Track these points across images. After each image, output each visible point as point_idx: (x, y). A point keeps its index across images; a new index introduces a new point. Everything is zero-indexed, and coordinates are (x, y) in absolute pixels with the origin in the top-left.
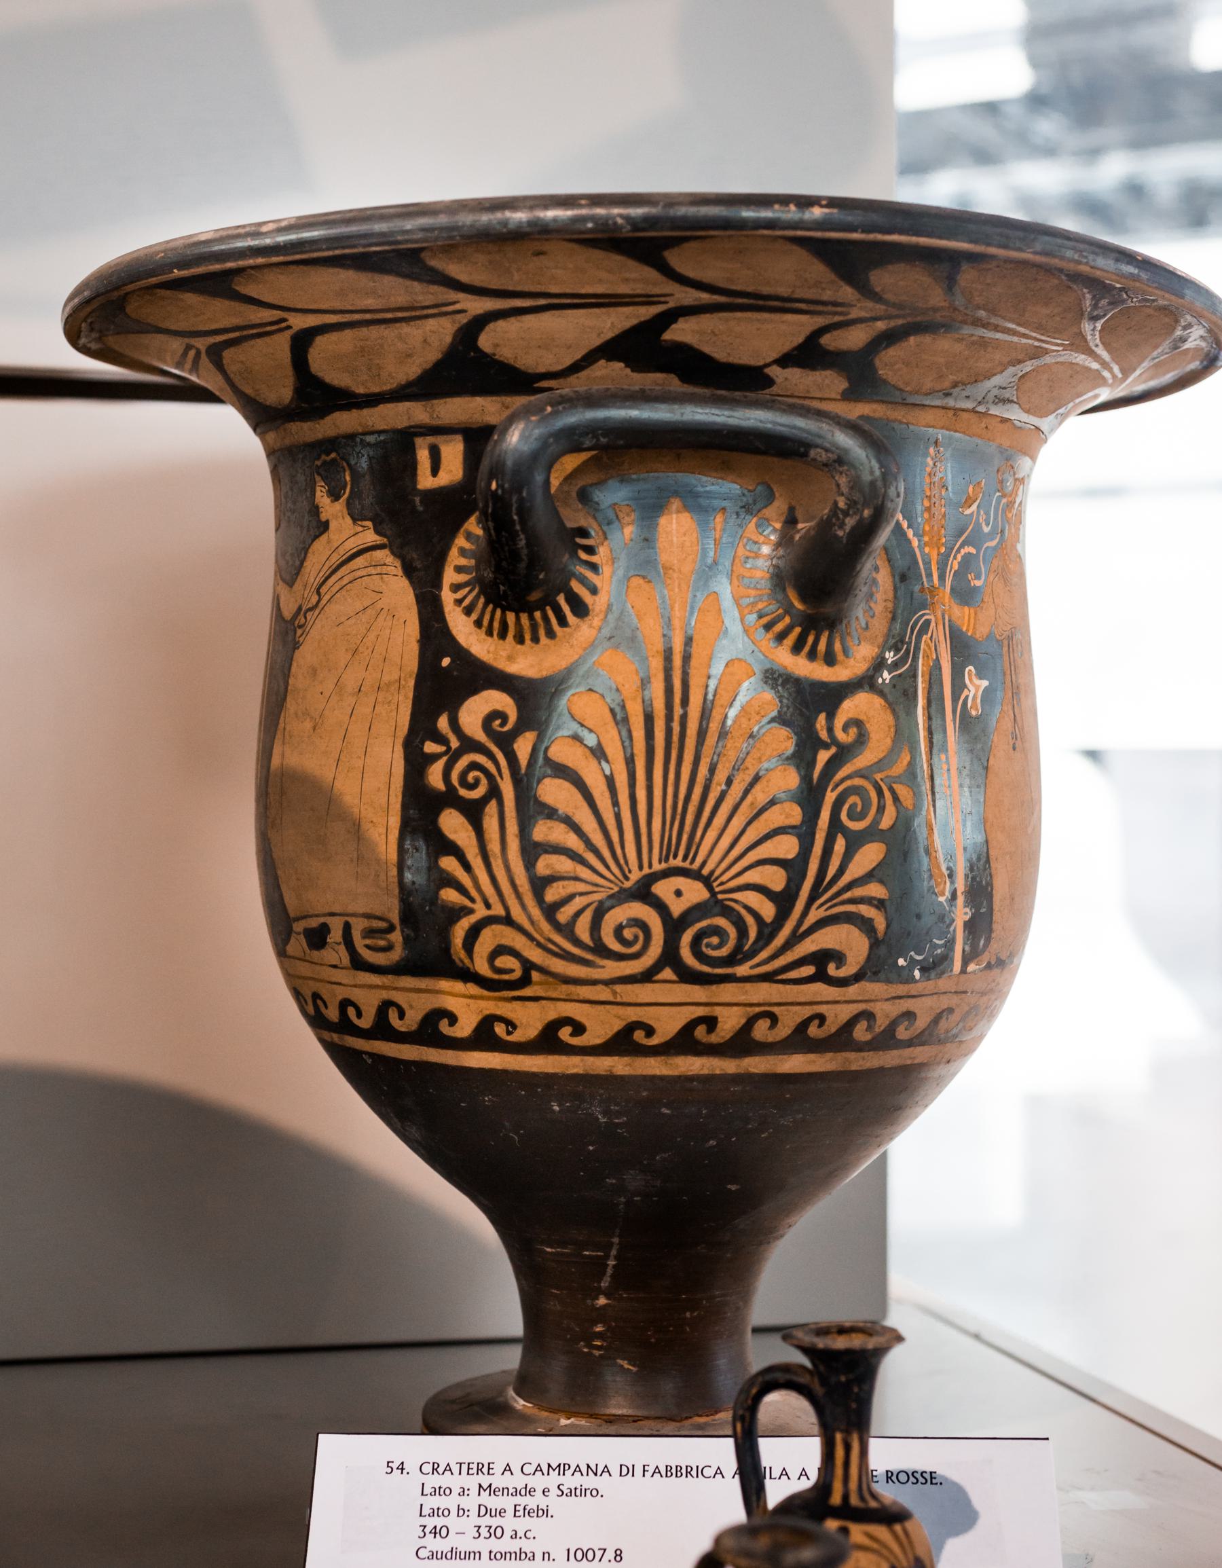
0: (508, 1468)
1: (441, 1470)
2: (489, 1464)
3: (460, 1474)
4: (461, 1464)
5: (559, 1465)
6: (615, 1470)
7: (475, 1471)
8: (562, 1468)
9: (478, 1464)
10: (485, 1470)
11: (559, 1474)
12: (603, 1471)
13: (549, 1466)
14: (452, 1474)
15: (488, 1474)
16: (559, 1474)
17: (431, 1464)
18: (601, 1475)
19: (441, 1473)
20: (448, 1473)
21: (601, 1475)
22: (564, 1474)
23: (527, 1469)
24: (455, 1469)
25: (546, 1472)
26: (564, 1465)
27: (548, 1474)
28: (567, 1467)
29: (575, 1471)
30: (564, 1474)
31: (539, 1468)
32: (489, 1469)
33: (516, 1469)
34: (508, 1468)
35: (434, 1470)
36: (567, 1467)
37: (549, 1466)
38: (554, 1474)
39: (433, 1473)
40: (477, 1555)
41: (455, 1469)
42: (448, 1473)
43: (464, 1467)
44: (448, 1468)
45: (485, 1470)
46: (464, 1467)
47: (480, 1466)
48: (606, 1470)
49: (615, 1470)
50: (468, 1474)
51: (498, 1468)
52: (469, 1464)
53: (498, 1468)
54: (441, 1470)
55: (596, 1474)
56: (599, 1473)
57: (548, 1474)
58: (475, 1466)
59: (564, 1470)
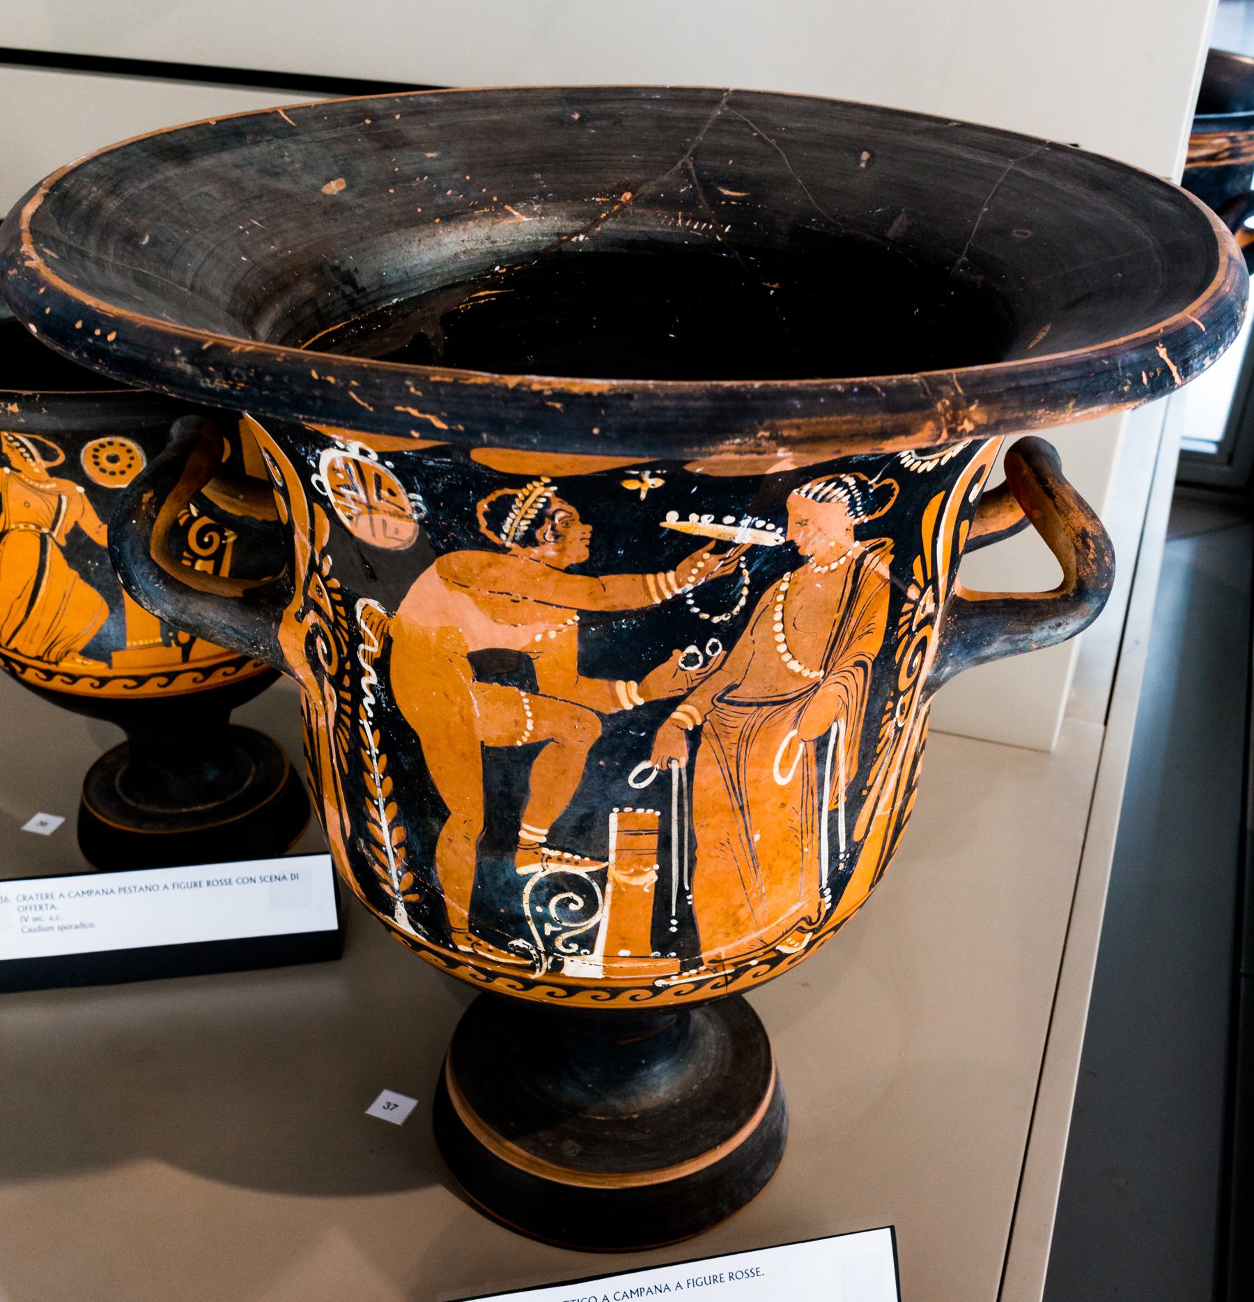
6: (116, 890)
23: (71, 895)
24: (34, 897)
33: (66, 895)
35: (24, 899)
40: (51, 928)
41: (34, 897)
43: (39, 897)
44: (31, 897)
49: (116, 890)
51: (56, 895)
53: (56, 895)
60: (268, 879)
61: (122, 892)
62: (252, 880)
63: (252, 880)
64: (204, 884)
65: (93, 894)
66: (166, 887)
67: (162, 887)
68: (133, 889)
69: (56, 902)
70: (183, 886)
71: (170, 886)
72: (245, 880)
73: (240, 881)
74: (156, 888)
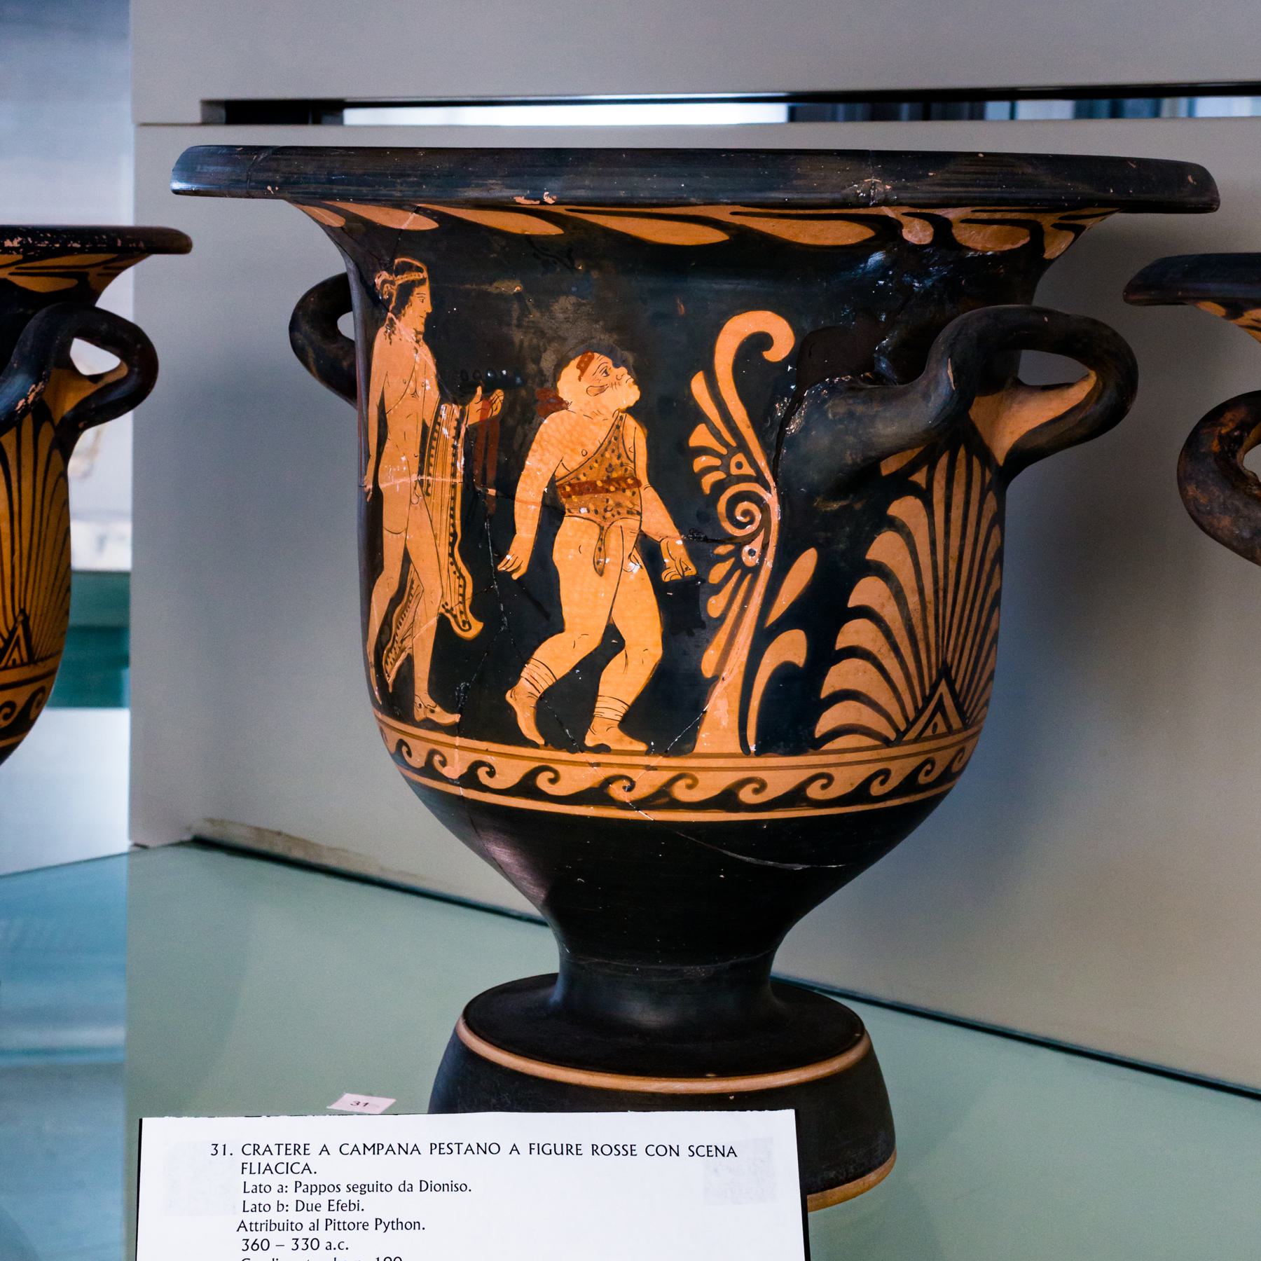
2: (305, 1145)
5: (374, 1146)
6: (424, 1148)
7: (292, 1151)
11: (374, 1154)
13: (365, 1146)
16: (374, 1154)
22: (378, 1154)
23: (346, 1149)
26: (378, 1145)
27: (364, 1154)
29: (388, 1150)
30: (378, 1154)
32: (305, 1149)
33: (334, 1149)
34: (325, 1149)
37: (365, 1146)
43: (283, 1148)
48: (416, 1149)
49: (424, 1148)
51: (314, 1149)
57: (364, 1154)
58: (292, 1147)
59: (378, 1150)
60: (703, 1151)
62: (673, 1151)
63: (673, 1151)
64: (587, 1150)
65: (382, 1152)
66: (515, 1148)
67: (506, 1148)
68: (455, 1148)
69: (313, 1159)
71: (524, 1149)
72: (661, 1150)
73: (652, 1150)
74: (495, 1149)
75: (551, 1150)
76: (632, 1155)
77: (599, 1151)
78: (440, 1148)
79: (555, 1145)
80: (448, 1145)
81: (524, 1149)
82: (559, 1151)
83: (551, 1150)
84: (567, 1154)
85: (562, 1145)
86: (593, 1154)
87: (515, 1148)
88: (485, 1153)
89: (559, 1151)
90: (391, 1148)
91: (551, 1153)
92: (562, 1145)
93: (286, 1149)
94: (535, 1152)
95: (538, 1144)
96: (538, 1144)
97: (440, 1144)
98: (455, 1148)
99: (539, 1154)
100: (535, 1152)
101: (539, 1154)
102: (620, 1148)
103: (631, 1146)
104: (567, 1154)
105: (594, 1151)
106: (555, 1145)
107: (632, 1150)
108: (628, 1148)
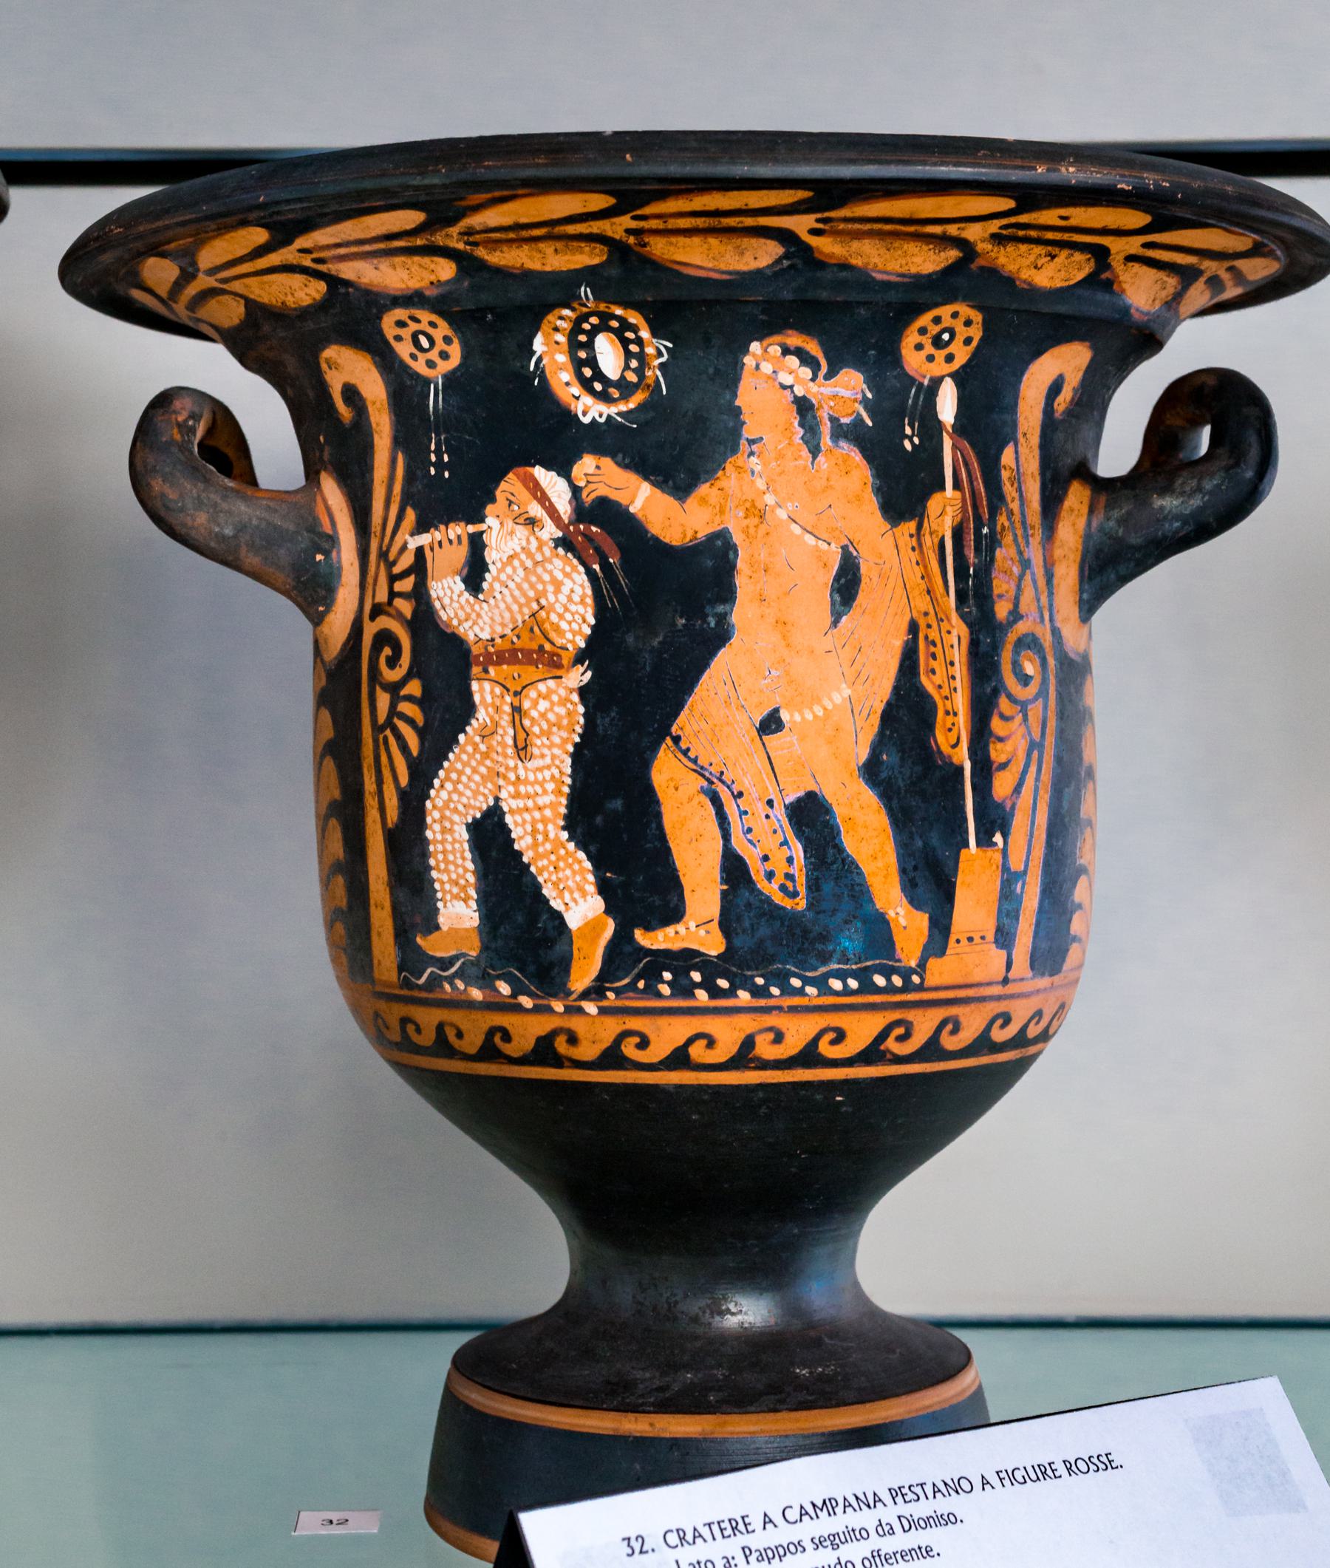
0: (767, 1520)
1: (689, 1537)
2: (743, 1518)
3: (714, 1539)
4: (709, 1525)
5: (824, 1502)
7: (729, 1532)
8: (828, 1505)
9: (730, 1520)
10: (741, 1527)
12: (875, 1502)
13: (814, 1505)
14: (705, 1541)
15: (748, 1532)
16: (830, 1515)
17: (675, 1533)
18: (875, 1506)
19: (691, 1541)
20: (699, 1541)
21: (875, 1506)
24: (705, 1532)
25: (814, 1515)
26: (830, 1500)
27: (818, 1517)
28: (834, 1504)
29: (845, 1507)
30: (835, 1513)
31: (803, 1513)
32: (746, 1525)
33: (777, 1518)
34: (767, 1520)
35: (682, 1539)
36: (834, 1504)
37: (814, 1505)
38: (823, 1514)
39: (682, 1545)
41: (705, 1532)
42: (699, 1541)
43: (715, 1528)
44: (697, 1535)
45: (741, 1527)
46: (715, 1528)
47: (734, 1524)
48: (877, 1500)
50: (724, 1537)
51: (756, 1522)
52: (719, 1523)
53: (756, 1522)
54: (689, 1537)
55: (869, 1506)
56: (872, 1505)
57: (818, 1517)
58: (726, 1525)
59: (833, 1508)
61: (899, 1499)
64: (1062, 1470)
65: (839, 1510)
66: (985, 1482)
67: (977, 1485)
68: (918, 1490)
70: (1018, 1475)
71: (994, 1480)
75: (1023, 1477)
76: (1112, 1468)
77: (1074, 1468)
78: (903, 1495)
79: (1025, 1468)
80: (910, 1487)
81: (994, 1480)
82: (1034, 1477)
83: (1023, 1477)
84: (1045, 1479)
85: (1033, 1467)
86: (1070, 1475)
87: (985, 1482)
88: (957, 1492)
89: (1034, 1477)
90: (847, 1505)
91: (1025, 1482)
92: (1033, 1467)
93: (721, 1530)
94: (1007, 1482)
95: (1006, 1471)
96: (1006, 1471)
97: (899, 1488)
98: (918, 1490)
99: (1012, 1484)
100: (1007, 1482)
101: (1012, 1484)
102: (1095, 1460)
103: (1106, 1455)
104: (1045, 1479)
105: (1069, 1469)
106: (1025, 1468)
107: (1110, 1462)
108: (1104, 1459)
